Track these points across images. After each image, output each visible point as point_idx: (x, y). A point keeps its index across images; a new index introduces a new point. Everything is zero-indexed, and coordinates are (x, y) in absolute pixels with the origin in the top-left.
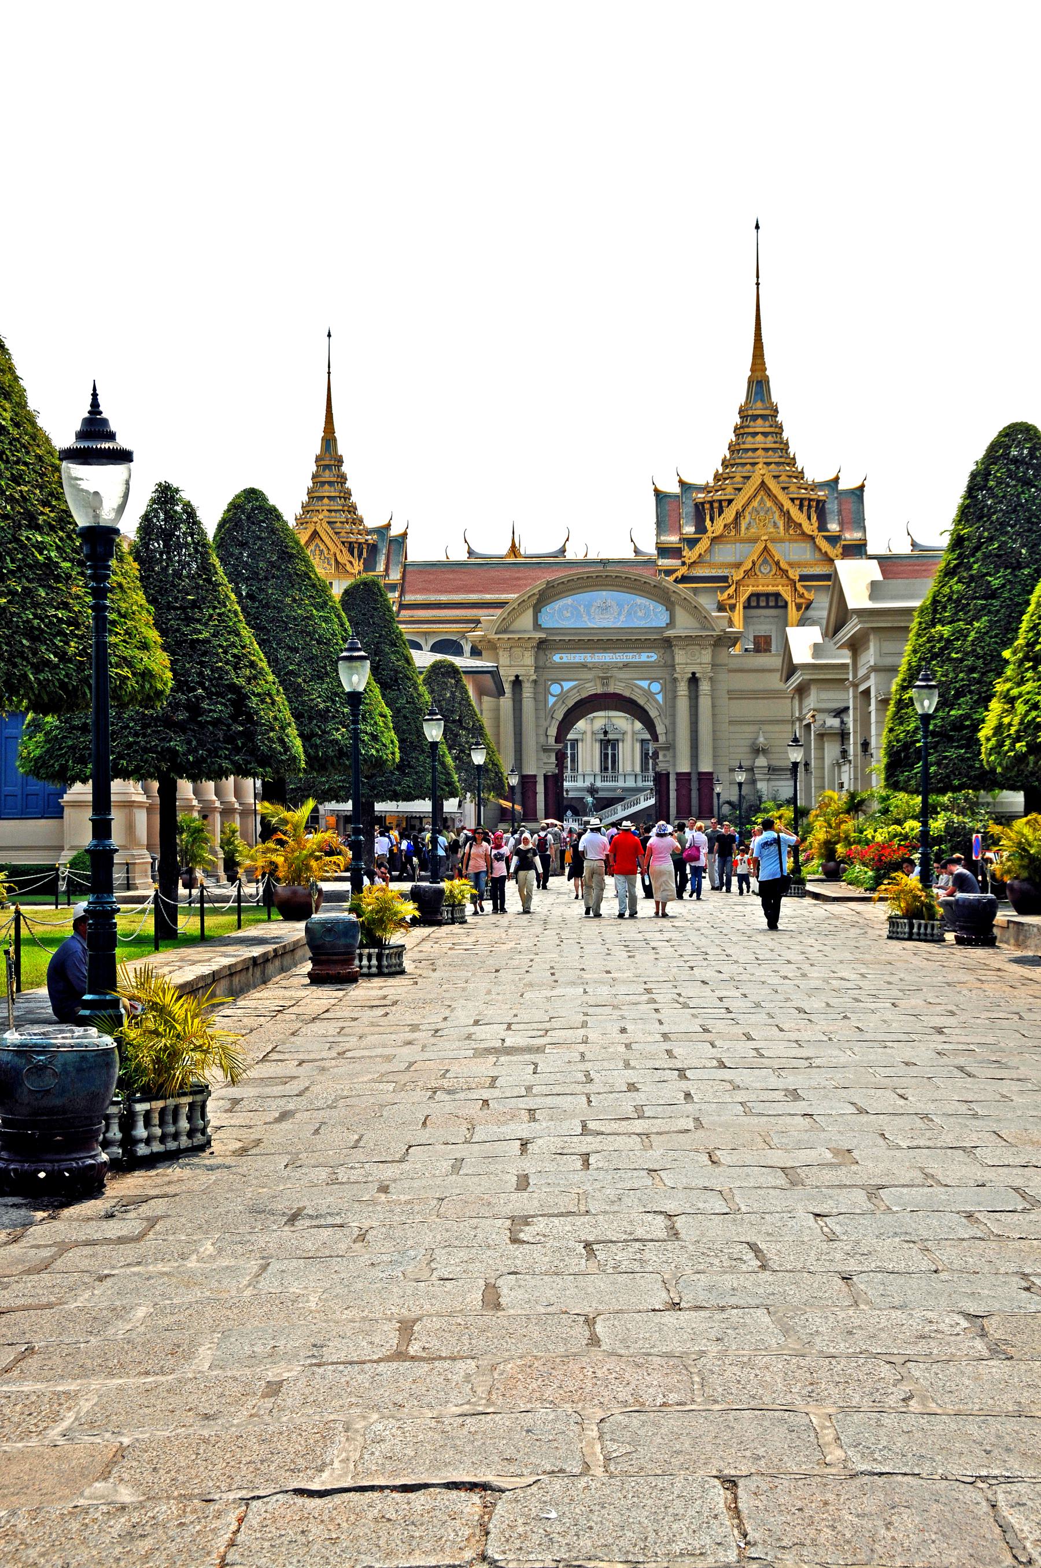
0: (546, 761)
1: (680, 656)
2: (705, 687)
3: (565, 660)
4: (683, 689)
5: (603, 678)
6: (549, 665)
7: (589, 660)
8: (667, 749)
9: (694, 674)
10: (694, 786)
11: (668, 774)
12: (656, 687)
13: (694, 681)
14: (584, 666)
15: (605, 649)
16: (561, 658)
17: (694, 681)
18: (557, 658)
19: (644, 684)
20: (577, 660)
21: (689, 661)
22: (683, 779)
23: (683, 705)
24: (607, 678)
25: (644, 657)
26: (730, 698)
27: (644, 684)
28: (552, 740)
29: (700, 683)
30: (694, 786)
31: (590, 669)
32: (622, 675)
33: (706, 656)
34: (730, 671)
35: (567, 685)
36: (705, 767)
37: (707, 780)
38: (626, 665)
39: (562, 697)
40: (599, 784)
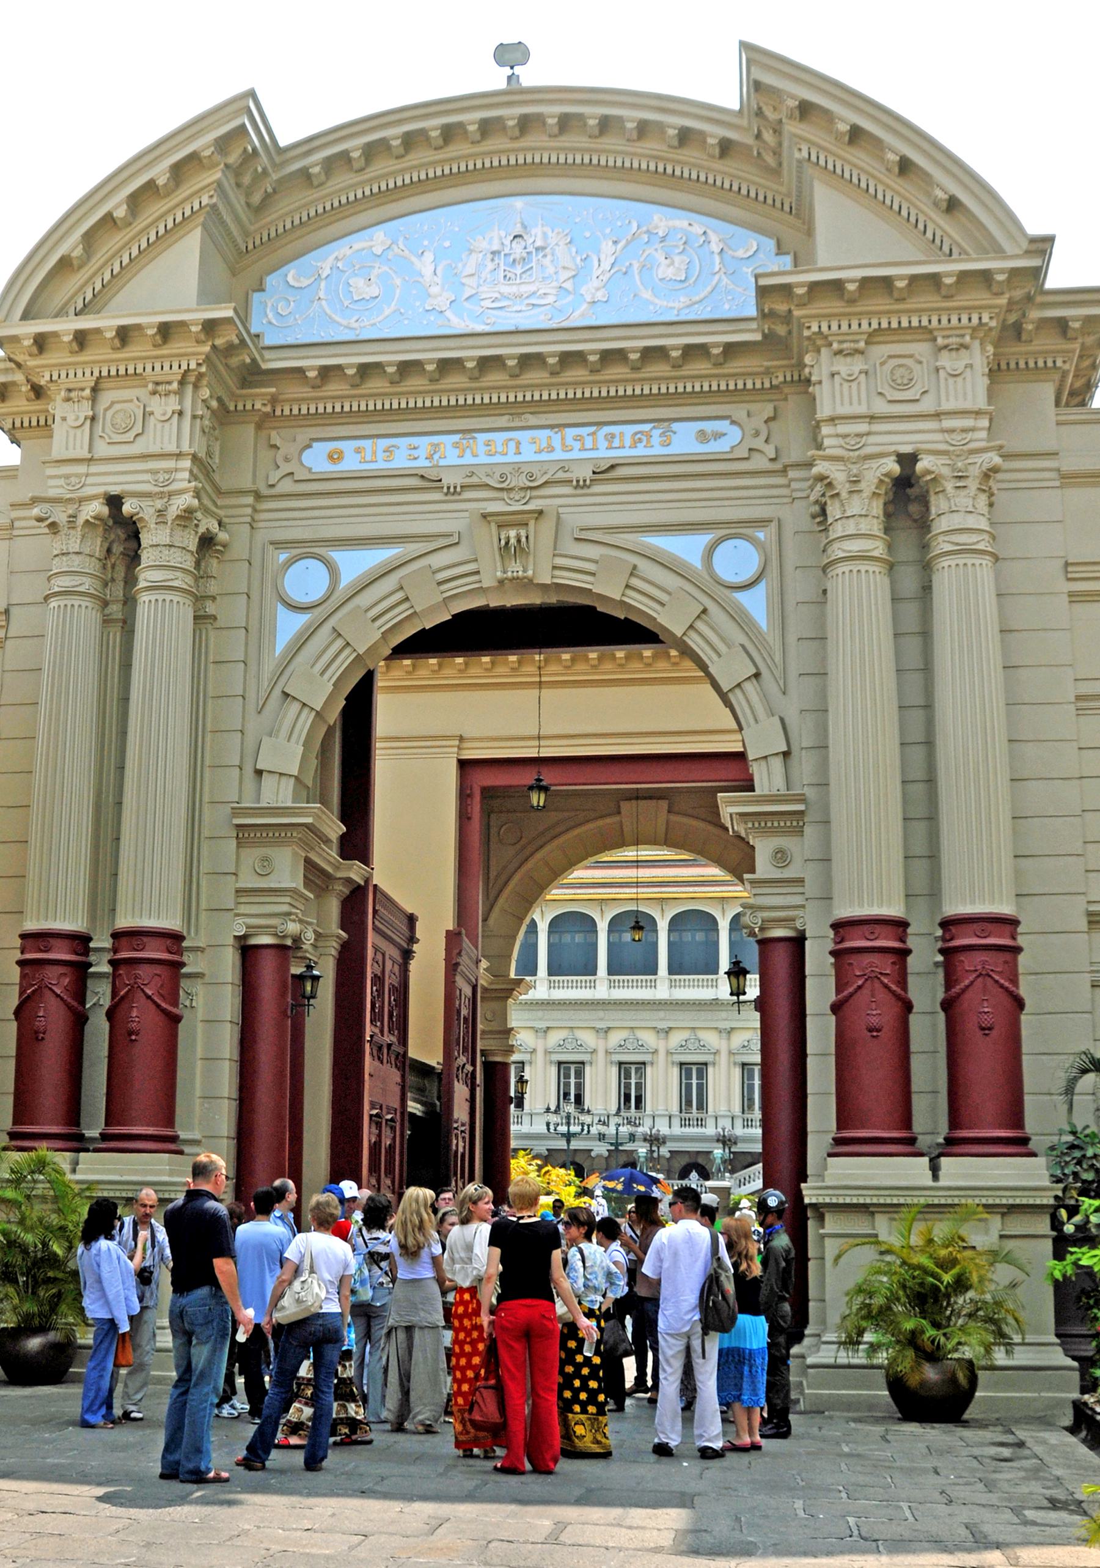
0: (248, 881)
1: (841, 388)
2: (956, 514)
3: (351, 463)
4: (860, 521)
5: (503, 522)
6: (287, 486)
7: (452, 458)
8: (792, 822)
9: (908, 460)
10: (925, 989)
11: (798, 942)
12: (737, 560)
13: (907, 493)
14: (429, 482)
15: (517, 412)
16: (335, 457)
17: (907, 493)
18: (316, 459)
19: (687, 548)
20: (401, 461)
21: (881, 407)
22: (871, 949)
23: (862, 598)
24: (519, 520)
25: (684, 439)
26: (1074, 597)
27: (687, 548)
28: (278, 794)
29: (937, 504)
30: (925, 989)
31: (452, 492)
32: (581, 513)
33: (966, 382)
34: (1069, 479)
35: (352, 565)
36: (975, 891)
37: (983, 952)
38: (606, 472)
39: (322, 611)
40: (739, 1131)
